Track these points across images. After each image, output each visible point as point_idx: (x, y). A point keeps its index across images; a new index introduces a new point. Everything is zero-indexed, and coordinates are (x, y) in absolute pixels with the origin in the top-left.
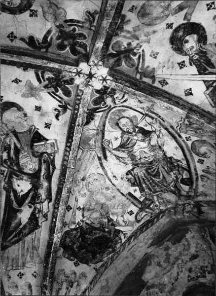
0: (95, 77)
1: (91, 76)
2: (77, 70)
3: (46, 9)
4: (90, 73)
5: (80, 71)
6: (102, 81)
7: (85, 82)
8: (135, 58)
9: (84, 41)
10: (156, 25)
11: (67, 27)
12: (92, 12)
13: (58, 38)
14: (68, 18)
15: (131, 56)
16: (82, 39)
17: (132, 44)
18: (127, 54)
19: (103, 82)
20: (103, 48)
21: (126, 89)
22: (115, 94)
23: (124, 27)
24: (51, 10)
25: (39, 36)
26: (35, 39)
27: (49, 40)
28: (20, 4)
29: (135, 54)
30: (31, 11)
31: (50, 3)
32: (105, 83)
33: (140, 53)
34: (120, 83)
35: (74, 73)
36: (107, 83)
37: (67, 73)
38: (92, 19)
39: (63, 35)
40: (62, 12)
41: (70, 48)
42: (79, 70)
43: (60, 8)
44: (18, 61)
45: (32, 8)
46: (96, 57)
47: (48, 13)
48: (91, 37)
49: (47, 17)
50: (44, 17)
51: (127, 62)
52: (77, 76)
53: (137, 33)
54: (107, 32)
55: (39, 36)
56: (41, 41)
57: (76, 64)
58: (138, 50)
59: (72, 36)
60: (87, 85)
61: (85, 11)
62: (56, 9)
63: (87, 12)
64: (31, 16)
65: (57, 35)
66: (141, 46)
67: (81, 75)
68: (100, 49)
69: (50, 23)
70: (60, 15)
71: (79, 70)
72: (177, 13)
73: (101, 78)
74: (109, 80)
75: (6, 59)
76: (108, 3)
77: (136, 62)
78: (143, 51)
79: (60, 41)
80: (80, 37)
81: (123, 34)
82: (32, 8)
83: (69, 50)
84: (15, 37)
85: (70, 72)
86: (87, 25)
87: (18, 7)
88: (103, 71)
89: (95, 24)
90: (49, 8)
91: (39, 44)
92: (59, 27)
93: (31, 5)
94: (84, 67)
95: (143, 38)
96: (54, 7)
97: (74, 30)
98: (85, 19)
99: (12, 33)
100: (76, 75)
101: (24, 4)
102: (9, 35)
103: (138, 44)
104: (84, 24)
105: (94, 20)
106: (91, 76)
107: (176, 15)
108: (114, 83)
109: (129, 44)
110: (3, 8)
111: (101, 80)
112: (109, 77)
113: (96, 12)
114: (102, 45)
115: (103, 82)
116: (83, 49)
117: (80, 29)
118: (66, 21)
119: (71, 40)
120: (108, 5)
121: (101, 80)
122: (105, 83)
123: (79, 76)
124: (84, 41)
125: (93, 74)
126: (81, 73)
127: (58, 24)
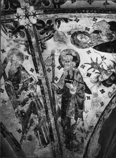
0: (24, 16)
1: (27, 16)
2: (36, 17)
3: (64, 37)
4: (28, 18)
5: (34, 17)
6: (19, 19)
7: (28, 10)
8: (8, 30)
9: (40, 31)
10: (10, 50)
11: (51, 34)
12: (44, 50)
13: (53, 25)
14: (52, 38)
15: (11, 30)
16: (41, 31)
17: (15, 38)
18: (14, 31)
19: (18, 15)
20: (30, 38)
21: (3, 18)
22: (4, 2)
23: (25, 47)
24: (61, 38)
25: (63, 23)
26: (64, 22)
27: (57, 23)
28: (77, 36)
29: (10, 32)
30: (71, 34)
31: (63, 41)
32: (17, 15)
33: (8, 33)
34: (9, 20)
35: (37, 14)
36: (16, 16)
37: (41, 13)
38: (43, 46)
39: (51, 28)
40: (56, 39)
41: (45, 23)
42: (35, 17)
43: (58, 41)
44: (71, 14)
45: (71, 35)
46: (31, 31)
47: (62, 35)
48: (38, 36)
49: (62, 33)
50: (63, 33)
51: (11, 26)
52: (34, 12)
53: (17, 44)
54: (34, 49)
55: (63, 23)
56: (61, 21)
57: (39, 21)
58: (10, 35)
59: (46, 30)
60: (25, 8)
61: (47, 48)
62: (60, 40)
63: (46, 48)
64: (70, 32)
65: (54, 27)
66: (10, 37)
67: (32, 14)
68: (32, 37)
69: (60, 31)
70: (57, 37)
71: (35, 17)
72: (5, 59)
73: (21, 17)
74: (16, 19)
75: (78, 14)
76: (41, 66)
77: (6, 29)
78: (7, 35)
79: (52, 24)
80: (43, 32)
81: (23, 42)
82: (71, 35)
83: (44, 21)
84: (75, 20)
85: (39, 14)
86: (43, 41)
87: (78, 35)
88: (22, 22)
89: (40, 45)
90: (63, 38)
91: (62, 20)
92: (54, 31)
93: (72, 37)
94: (34, 21)
95: (12, 42)
96: (61, 40)
97: (47, 34)
98: (45, 44)
99: (77, 22)
100: (35, 13)
101: (75, 36)
102: (79, 21)
103: (12, 38)
104: (44, 40)
105: (41, 47)
106: (27, 16)
107: (4, 58)
108: (12, 18)
109: (17, 37)
110: (84, 33)
111: (20, 16)
112: (17, 20)
113: (42, 51)
114: (32, 40)
115: (18, 15)
116: (38, 26)
117: (45, 37)
118: (53, 36)
119: (46, 27)
120: (41, 65)
121: (20, 16)
122: (17, 15)
123: (33, 13)
124: (40, 31)
125: (27, 18)
126: (33, 15)
127: (56, 32)
